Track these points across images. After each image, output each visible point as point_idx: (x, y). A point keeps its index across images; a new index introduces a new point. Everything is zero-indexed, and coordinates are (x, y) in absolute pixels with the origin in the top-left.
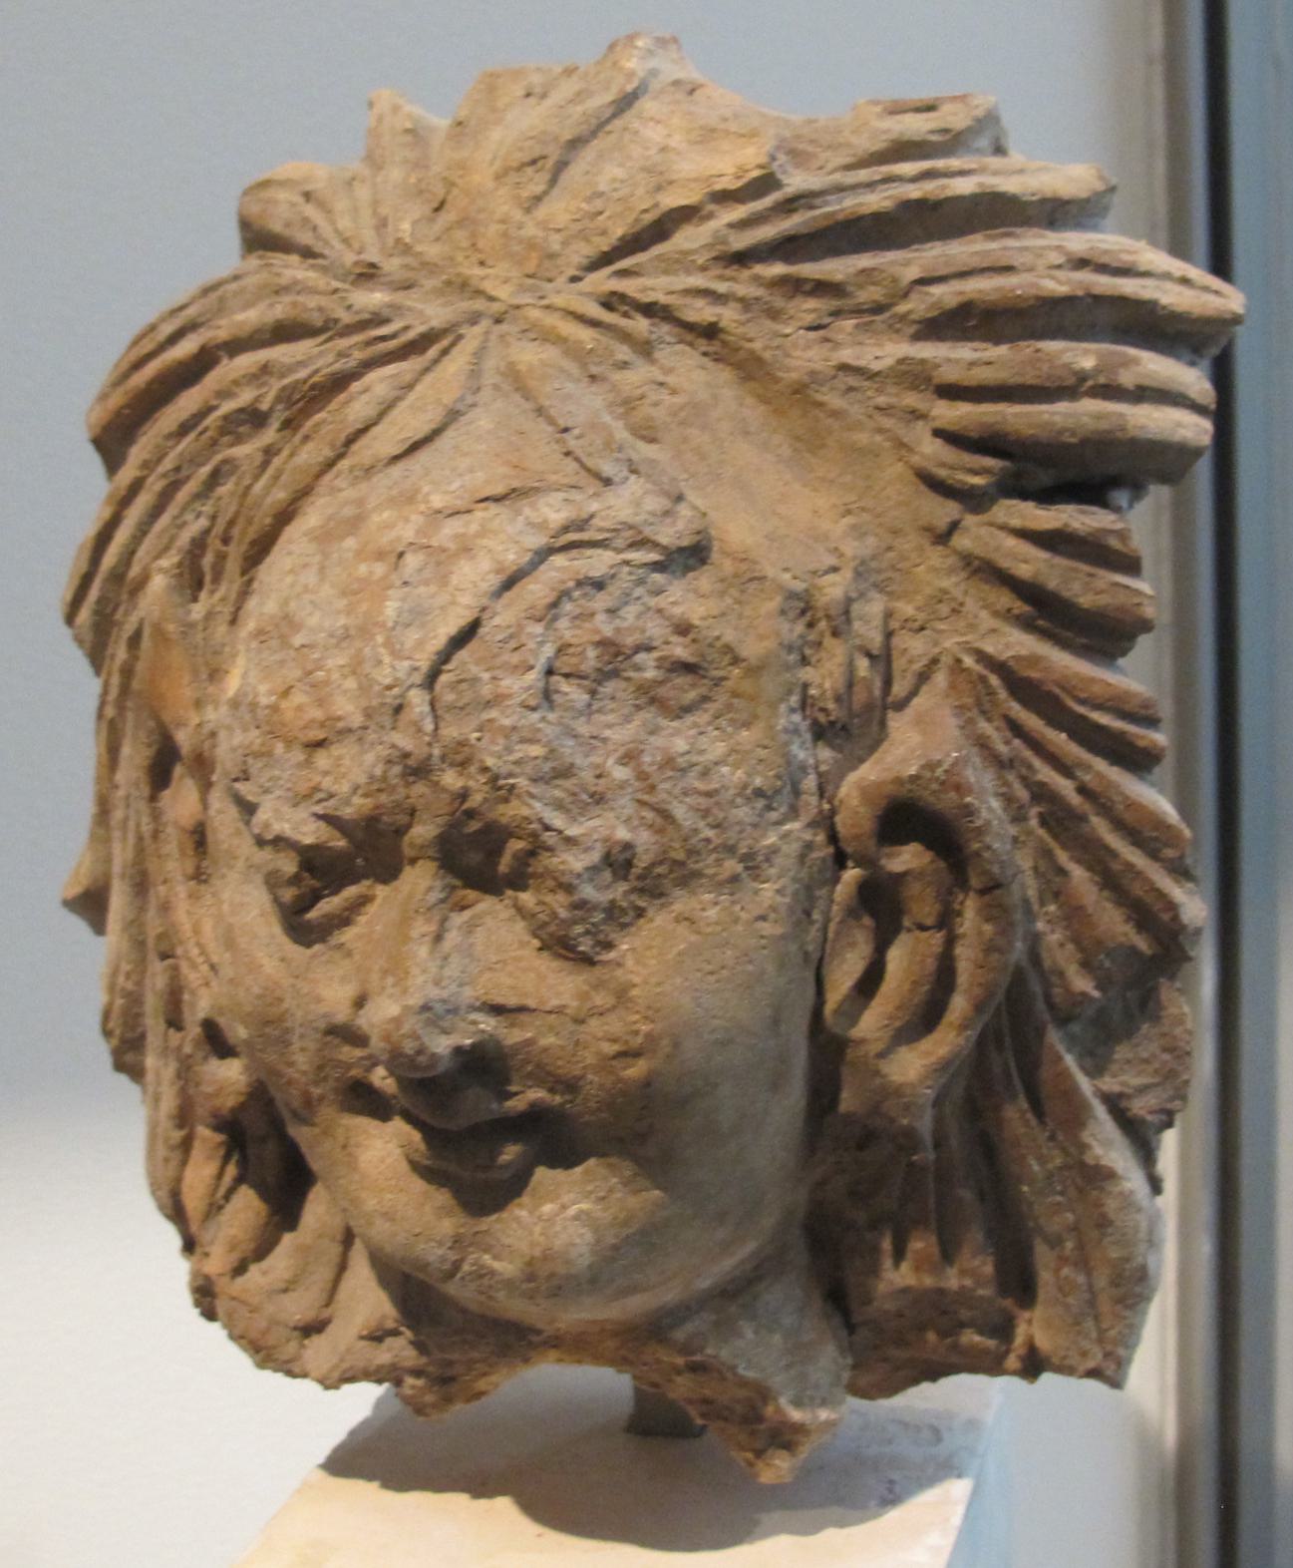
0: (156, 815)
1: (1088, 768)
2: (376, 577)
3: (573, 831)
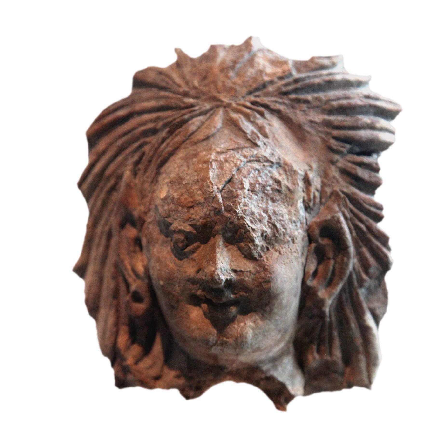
1: (367, 221)
2: (204, 167)
3: (254, 227)
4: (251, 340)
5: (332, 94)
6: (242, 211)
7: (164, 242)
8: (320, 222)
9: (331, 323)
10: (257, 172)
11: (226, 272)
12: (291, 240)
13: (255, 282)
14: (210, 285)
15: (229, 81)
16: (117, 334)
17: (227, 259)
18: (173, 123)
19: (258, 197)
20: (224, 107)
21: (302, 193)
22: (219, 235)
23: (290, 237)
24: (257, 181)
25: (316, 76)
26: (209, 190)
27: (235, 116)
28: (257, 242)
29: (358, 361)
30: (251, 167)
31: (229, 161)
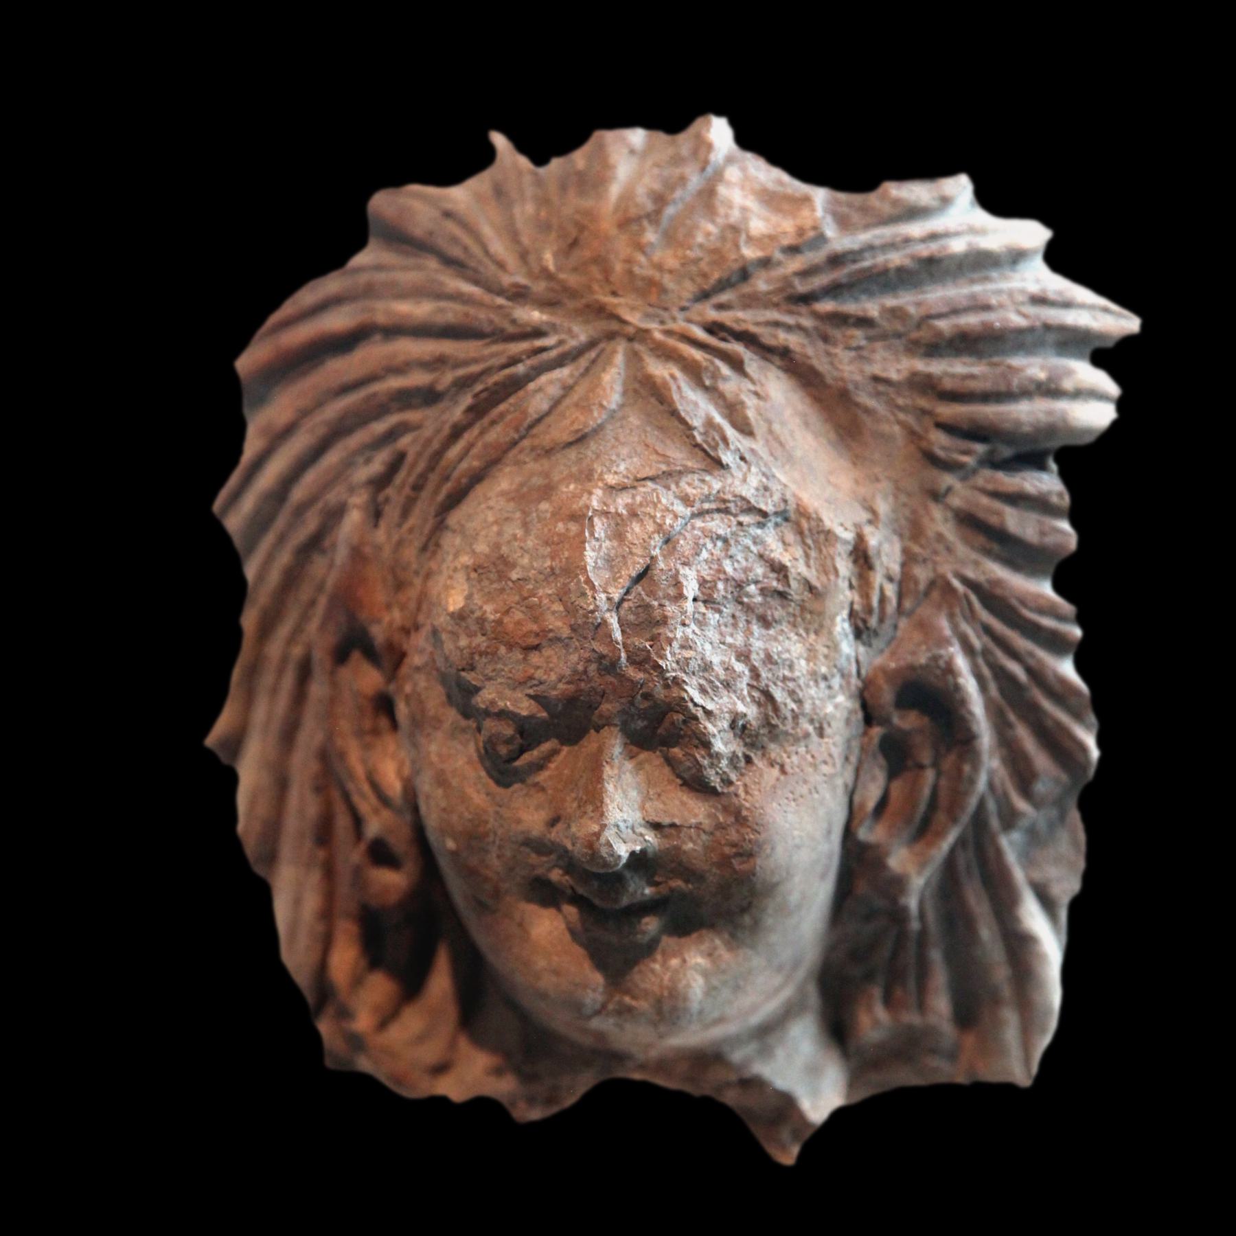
1: (1031, 654)
2: (572, 534)
3: (710, 706)
4: (700, 1002)
5: (937, 295)
6: (678, 662)
7: (455, 732)
8: (898, 671)
9: (923, 932)
10: (719, 544)
12: (815, 728)
13: (712, 855)
14: (588, 868)
15: (642, 259)
16: (327, 943)
17: (634, 794)
19: (723, 617)
20: (630, 339)
21: (848, 593)
22: (612, 729)
23: (812, 721)
24: (721, 570)
25: (891, 246)
26: (585, 606)
27: (659, 370)
28: (719, 746)
29: (998, 1024)
30: (703, 530)
31: (641, 517)
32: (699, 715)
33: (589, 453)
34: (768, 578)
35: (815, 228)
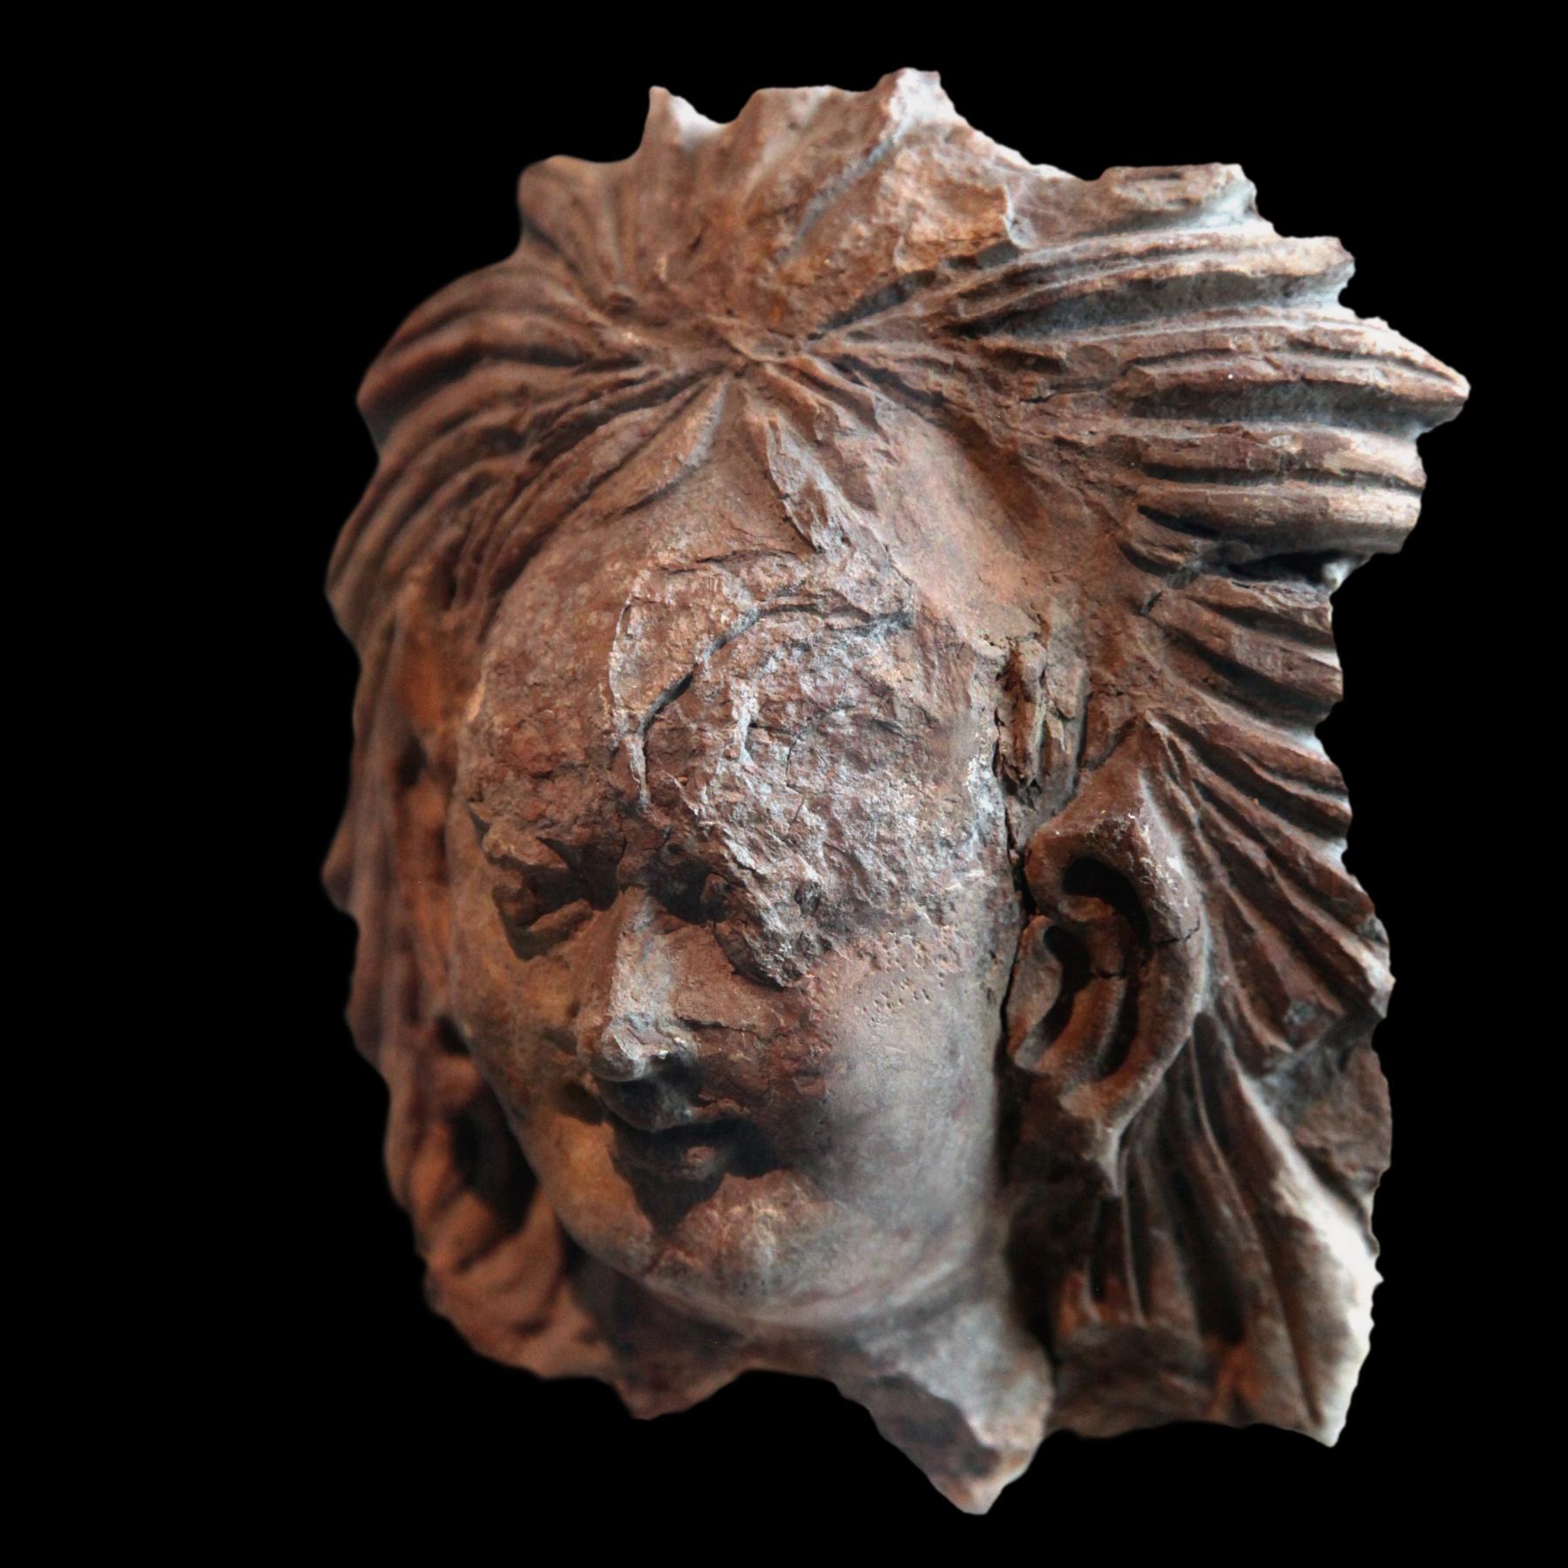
0: (403, 813)
1: (1277, 832)
2: (603, 628)
3: (763, 870)
4: (772, 1267)
5: (1155, 331)
6: (717, 807)
8: (1061, 840)
10: (797, 653)
11: (650, 1028)
12: (929, 910)
17: (664, 980)
18: (563, 418)
21: (991, 731)
23: (922, 901)
25: (1096, 262)
26: (600, 724)
27: (760, 415)
28: (775, 923)
30: (773, 632)
32: (745, 881)
33: (650, 522)
34: (865, 702)
35: (995, 235)
